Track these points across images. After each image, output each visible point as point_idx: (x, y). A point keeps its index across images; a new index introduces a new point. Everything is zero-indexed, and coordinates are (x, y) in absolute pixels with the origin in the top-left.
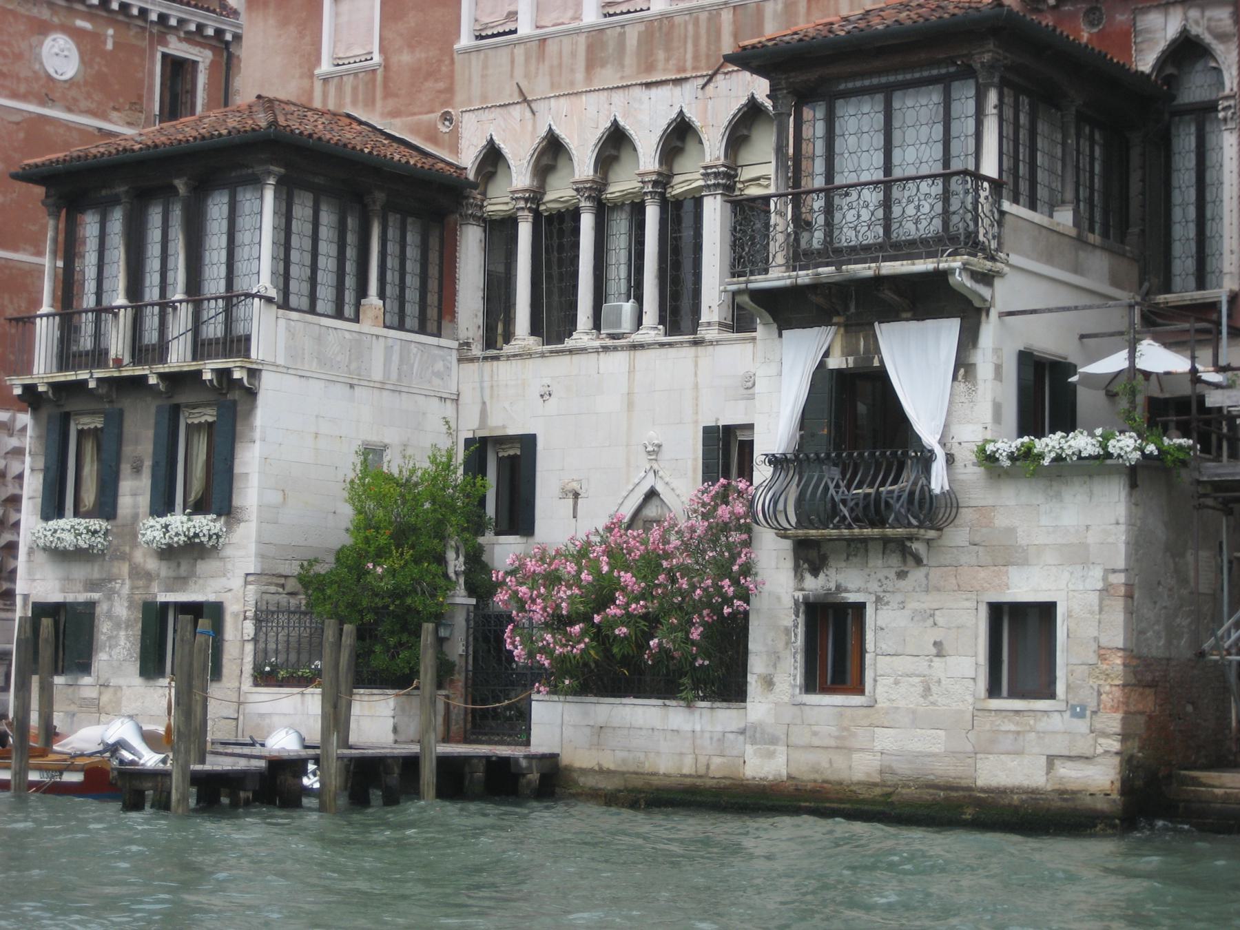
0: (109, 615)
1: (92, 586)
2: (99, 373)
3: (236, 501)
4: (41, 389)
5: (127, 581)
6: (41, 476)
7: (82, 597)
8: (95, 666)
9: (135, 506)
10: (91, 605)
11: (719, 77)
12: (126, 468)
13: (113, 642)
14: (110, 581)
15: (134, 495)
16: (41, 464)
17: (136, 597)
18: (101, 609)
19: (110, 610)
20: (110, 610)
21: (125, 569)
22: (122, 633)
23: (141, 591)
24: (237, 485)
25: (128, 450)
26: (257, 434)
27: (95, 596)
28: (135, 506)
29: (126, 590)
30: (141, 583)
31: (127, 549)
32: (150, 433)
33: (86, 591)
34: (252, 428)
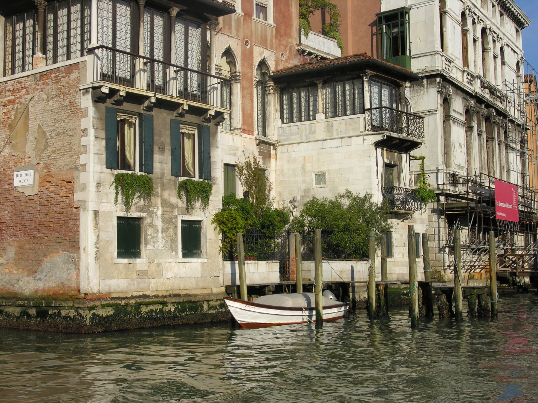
0: (151, 225)
1: (142, 210)
2: (159, 96)
3: (213, 175)
5: (160, 208)
6: (104, 143)
9: (162, 169)
10: (139, 219)
11: (219, 34)
13: (155, 240)
15: (161, 163)
16: (103, 134)
18: (147, 221)
19: (151, 223)
20: (151, 223)
21: (159, 201)
22: (160, 235)
23: (168, 213)
24: (212, 166)
25: (156, 138)
26: (219, 144)
27: (143, 215)
28: (162, 169)
29: (160, 213)
31: (159, 191)
32: (168, 132)
34: (217, 141)
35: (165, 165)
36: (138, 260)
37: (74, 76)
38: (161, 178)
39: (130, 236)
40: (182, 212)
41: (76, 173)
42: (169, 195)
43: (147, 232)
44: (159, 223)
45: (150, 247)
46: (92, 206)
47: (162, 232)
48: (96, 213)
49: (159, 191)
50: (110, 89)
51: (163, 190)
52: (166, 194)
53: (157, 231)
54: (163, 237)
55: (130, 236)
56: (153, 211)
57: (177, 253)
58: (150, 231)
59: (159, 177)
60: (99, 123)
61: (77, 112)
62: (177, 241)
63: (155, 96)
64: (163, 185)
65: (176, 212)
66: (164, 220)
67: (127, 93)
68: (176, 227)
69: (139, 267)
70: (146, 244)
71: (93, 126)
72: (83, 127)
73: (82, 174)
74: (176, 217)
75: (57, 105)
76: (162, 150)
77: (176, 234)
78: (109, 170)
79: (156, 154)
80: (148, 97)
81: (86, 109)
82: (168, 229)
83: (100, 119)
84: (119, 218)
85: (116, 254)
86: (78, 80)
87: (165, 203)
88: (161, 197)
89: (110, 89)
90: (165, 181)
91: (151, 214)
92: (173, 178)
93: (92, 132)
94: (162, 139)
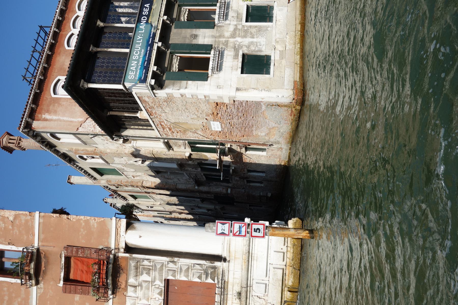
0: (248, 47)
2: (157, 39)
4: (155, 69)
6: (190, 82)
7: (240, 59)
8: (267, 53)
12: (195, 42)
13: (258, 44)
14: (235, 47)
16: (184, 82)
17: (243, 34)
21: (231, 40)
22: (255, 40)
23: (240, 32)
25: (187, 42)
27: (241, 53)
29: (239, 39)
30: (238, 33)
31: (224, 39)
33: (238, 58)
35: (206, 35)
36: (272, 58)
37: (147, 99)
38: (215, 37)
39: (255, 64)
40: (239, 21)
41: (211, 101)
42: (228, 31)
43: (253, 50)
44: (246, 41)
45: (263, 49)
46: (233, 93)
47: (253, 38)
48: (238, 89)
49: (224, 39)
50: (152, 78)
51: (224, 37)
52: (227, 34)
53: (252, 42)
54: (257, 37)
55: (255, 64)
56: (239, 45)
57: (269, 27)
58: (253, 48)
59: (214, 39)
60: (176, 86)
61: (169, 99)
62: (261, 27)
63: (157, 43)
64: (220, 36)
65: (240, 27)
66: (245, 37)
67: (155, 65)
68: (250, 27)
69: (277, 57)
70: (261, 51)
71: (178, 90)
72: (180, 96)
73: (211, 98)
74: (243, 26)
75: (168, 109)
76: (195, 36)
77: (256, 27)
78: (209, 79)
79: (198, 41)
80: (158, 47)
81: (167, 94)
82: (251, 33)
83: (173, 84)
84: (242, 73)
85: (267, 76)
86: (148, 97)
87: (233, 35)
88: (229, 38)
89: (152, 78)
90: (217, 35)
91: (240, 47)
92: (215, 27)
93: (182, 91)
94: (188, 36)
